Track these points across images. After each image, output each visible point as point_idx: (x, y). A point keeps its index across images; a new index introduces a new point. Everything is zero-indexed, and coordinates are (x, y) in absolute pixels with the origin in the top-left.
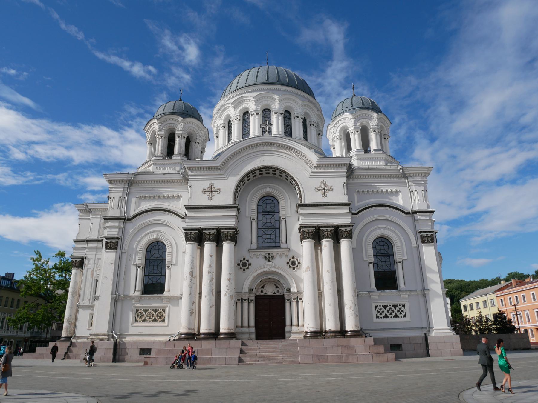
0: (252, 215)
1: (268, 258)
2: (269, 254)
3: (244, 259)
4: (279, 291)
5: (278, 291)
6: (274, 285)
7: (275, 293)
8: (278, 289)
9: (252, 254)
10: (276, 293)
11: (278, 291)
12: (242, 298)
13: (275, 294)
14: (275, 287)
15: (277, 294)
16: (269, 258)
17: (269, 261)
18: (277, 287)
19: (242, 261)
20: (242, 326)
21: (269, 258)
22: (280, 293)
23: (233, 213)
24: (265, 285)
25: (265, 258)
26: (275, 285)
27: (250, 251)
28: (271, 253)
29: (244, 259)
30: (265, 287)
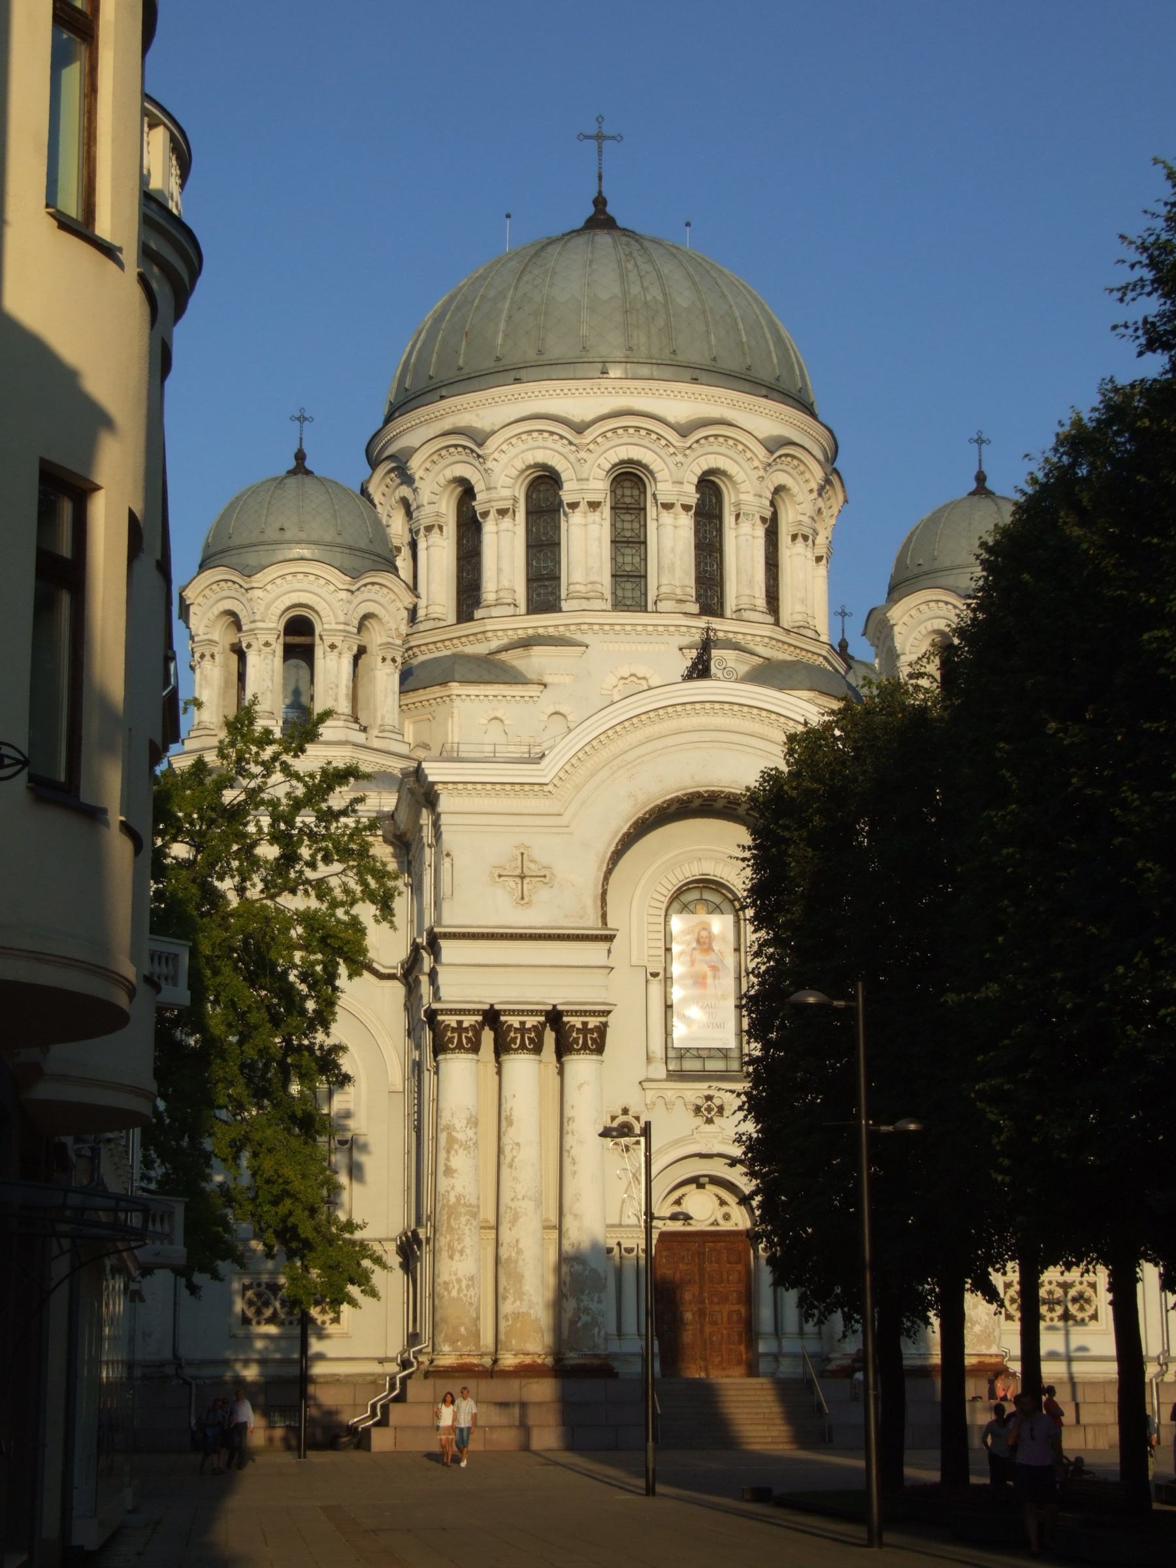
0: (651, 959)
1: (706, 1113)
2: (709, 1098)
3: (625, 1111)
4: (729, 1216)
5: (727, 1217)
6: (715, 1199)
7: (715, 1223)
8: (725, 1209)
9: (650, 1094)
10: (721, 1221)
11: (727, 1217)
12: (619, 1244)
13: (718, 1224)
14: (717, 1202)
15: (726, 1226)
16: (709, 1113)
17: (710, 1121)
18: (723, 1203)
19: (617, 1117)
20: (620, 1333)
21: (709, 1113)
22: (732, 1222)
23: (594, 953)
24: (683, 1195)
25: (698, 1109)
26: (717, 1196)
27: (646, 1085)
28: (717, 1094)
29: (625, 1111)
30: (684, 1202)
